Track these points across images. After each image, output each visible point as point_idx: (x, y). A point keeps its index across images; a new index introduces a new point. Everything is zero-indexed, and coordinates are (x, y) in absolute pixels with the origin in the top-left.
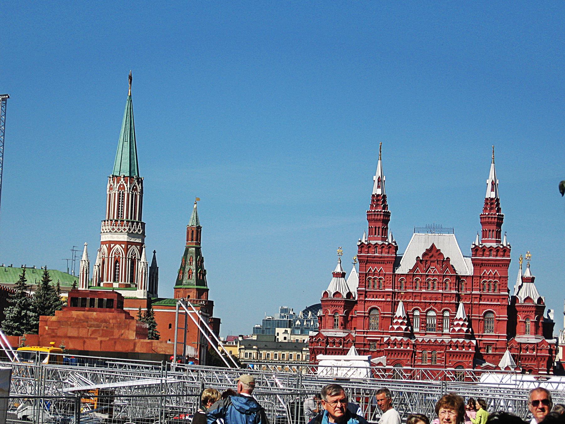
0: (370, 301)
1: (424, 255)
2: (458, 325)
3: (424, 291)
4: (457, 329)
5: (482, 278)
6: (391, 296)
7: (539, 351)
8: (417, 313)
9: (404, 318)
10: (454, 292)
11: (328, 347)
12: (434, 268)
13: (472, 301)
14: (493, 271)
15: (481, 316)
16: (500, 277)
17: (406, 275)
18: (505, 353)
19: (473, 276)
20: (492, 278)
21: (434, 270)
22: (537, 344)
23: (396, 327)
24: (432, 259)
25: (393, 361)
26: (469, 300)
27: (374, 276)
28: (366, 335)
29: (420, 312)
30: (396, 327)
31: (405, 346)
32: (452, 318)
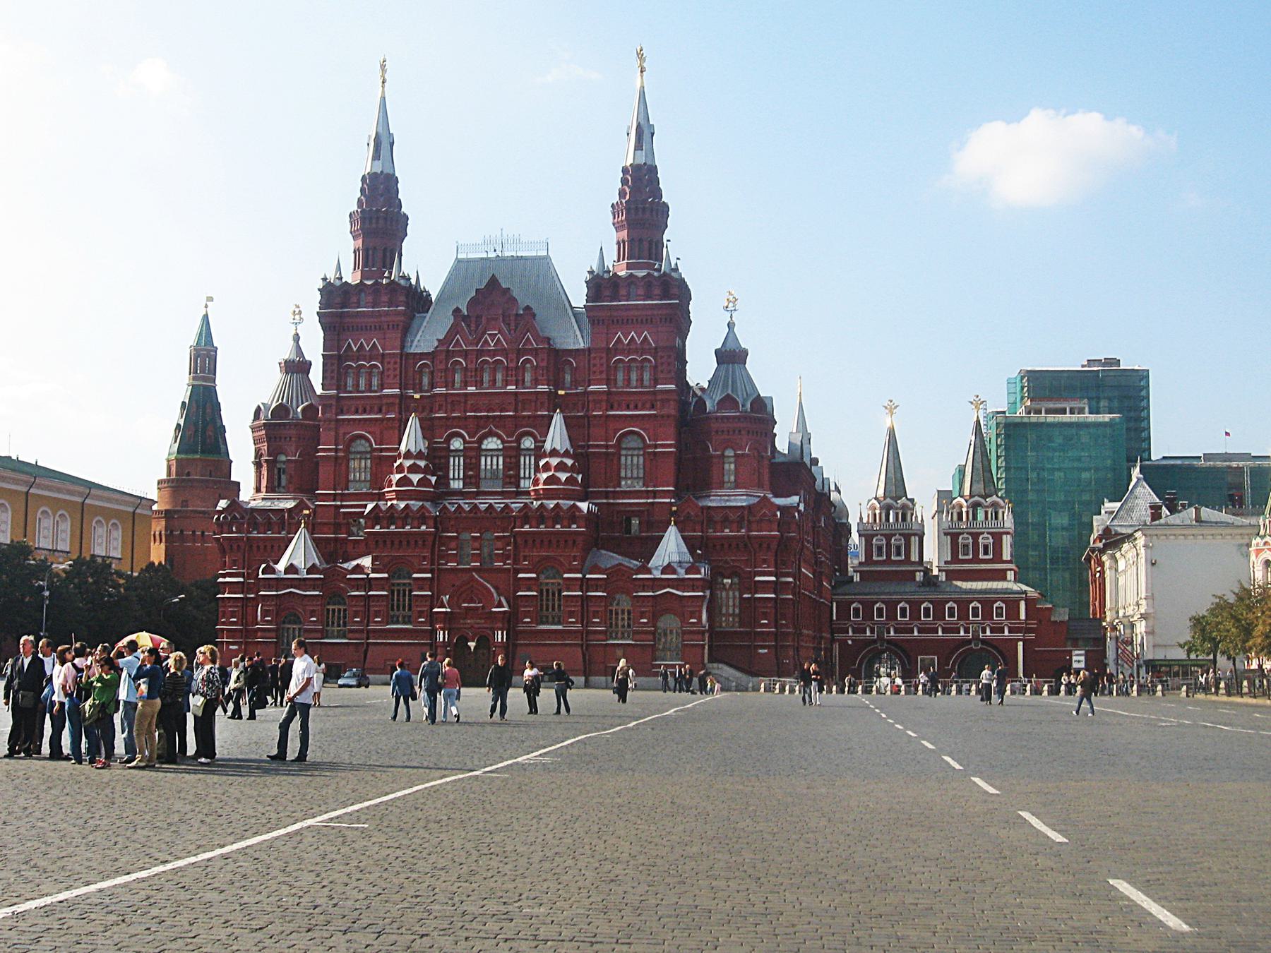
2: (547, 467)
3: (472, 389)
5: (613, 352)
6: (397, 406)
7: (754, 526)
10: (543, 388)
11: (255, 534)
12: (496, 335)
13: (587, 411)
15: (611, 446)
18: (667, 534)
19: (589, 349)
20: (636, 351)
21: (494, 337)
25: (386, 560)
26: (583, 408)
27: (358, 360)
28: (339, 503)
29: (465, 442)
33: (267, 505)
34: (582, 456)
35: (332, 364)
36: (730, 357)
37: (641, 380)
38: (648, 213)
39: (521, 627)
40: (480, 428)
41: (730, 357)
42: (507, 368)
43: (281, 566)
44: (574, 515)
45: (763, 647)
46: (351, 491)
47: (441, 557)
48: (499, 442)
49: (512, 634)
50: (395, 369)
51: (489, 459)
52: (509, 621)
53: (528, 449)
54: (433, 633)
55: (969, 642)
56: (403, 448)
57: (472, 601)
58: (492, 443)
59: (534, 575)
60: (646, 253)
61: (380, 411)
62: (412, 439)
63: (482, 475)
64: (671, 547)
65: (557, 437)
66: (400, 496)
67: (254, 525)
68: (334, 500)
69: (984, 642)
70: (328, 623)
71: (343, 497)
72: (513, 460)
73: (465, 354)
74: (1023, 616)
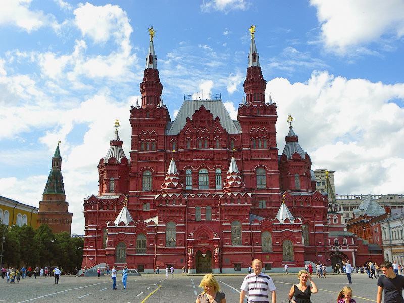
0: (143, 162)
1: (194, 116)
2: (231, 179)
4: (230, 183)
6: (163, 157)
7: (314, 204)
8: (189, 171)
9: (176, 175)
11: (102, 210)
14: (262, 128)
16: (269, 134)
17: (178, 136)
20: (261, 135)
21: (203, 129)
22: (311, 196)
23: (167, 184)
24: (203, 119)
29: (192, 170)
30: (167, 184)
31: (178, 202)
32: (224, 174)
33: (107, 197)
34: (243, 174)
35: (136, 140)
36: (291, 139)
37: (263, 146)
38: (260, 83)
39: (225, 247)
40: (199, 165)
41: (291, 139)
42: (192, 142)
43: (116, 222)
44: (246, 199)
45: (321, 254)
46: (144, 191)
47: (188, 217)
48: (206, 171)
49: (222, 249)
50: (162, 142)
51: (202, 178)
52: (220, 244)
53: (218, 173)
54: (186, 250)
55: (334, 253)
56: (169, 172)
57: (203, 235)
58: (204, 171)
59: (230, 224)
60: (260, 99)
61: (156, 159)
62: (172, 169)
63: (200, 184)
64: (283, 214)
65: (233, 167)
66: (169, 192)
67: (101, 205)
68: (137, 195)
69: (339, 252)
70: (138, 247)
71: (140, 193)
72: (213, 178)
73: (192, 135)
74: (353, 243)
